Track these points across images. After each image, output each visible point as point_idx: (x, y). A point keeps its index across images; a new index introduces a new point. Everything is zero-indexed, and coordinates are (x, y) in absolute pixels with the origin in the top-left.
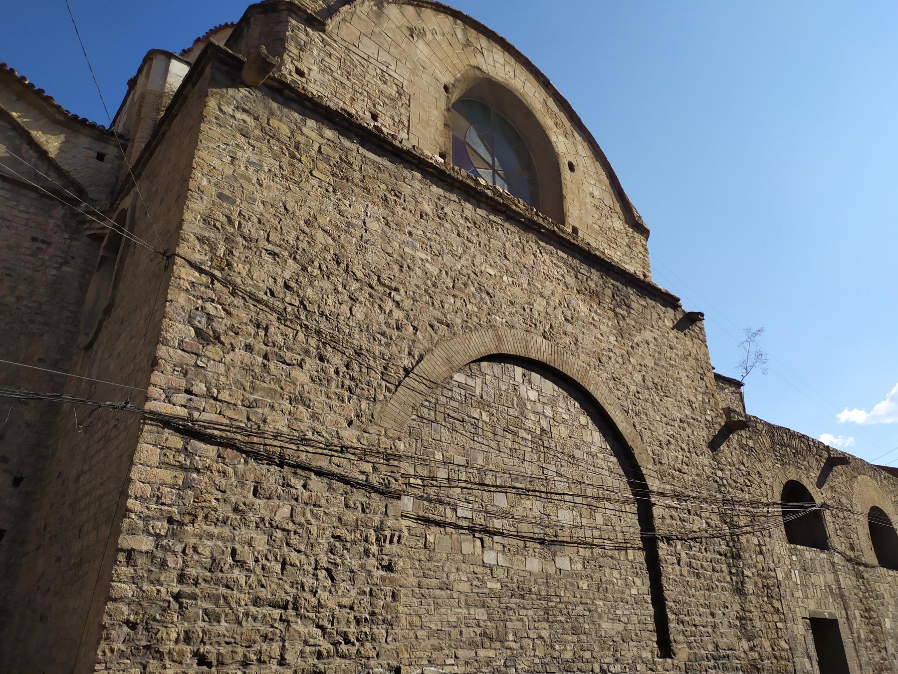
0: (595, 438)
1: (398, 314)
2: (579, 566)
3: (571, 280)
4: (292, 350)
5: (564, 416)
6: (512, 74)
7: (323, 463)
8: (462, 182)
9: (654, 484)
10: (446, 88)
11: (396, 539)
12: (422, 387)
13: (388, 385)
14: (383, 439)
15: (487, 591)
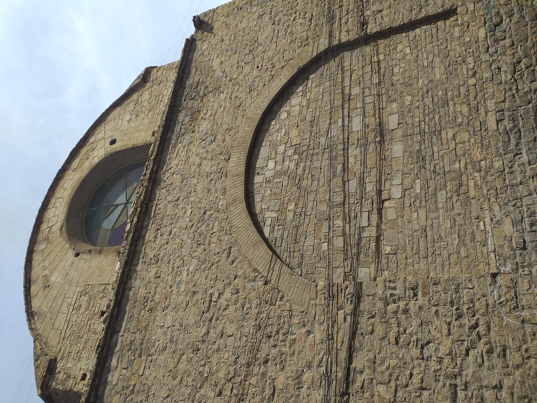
0: (295, 101)
1: (227, 295)
2: (395, 105)
3: (186, 139)
4: (263, 388)
5: (283, 134)
6: (61, 200)
7: (343, 355)
8: (131, 246)
9: (323, 44)
10: (77, 255)
11: (392, 285)
12: (277, 267)
13: (278, 299)
14: (318, 301)
15: (423, 192)
